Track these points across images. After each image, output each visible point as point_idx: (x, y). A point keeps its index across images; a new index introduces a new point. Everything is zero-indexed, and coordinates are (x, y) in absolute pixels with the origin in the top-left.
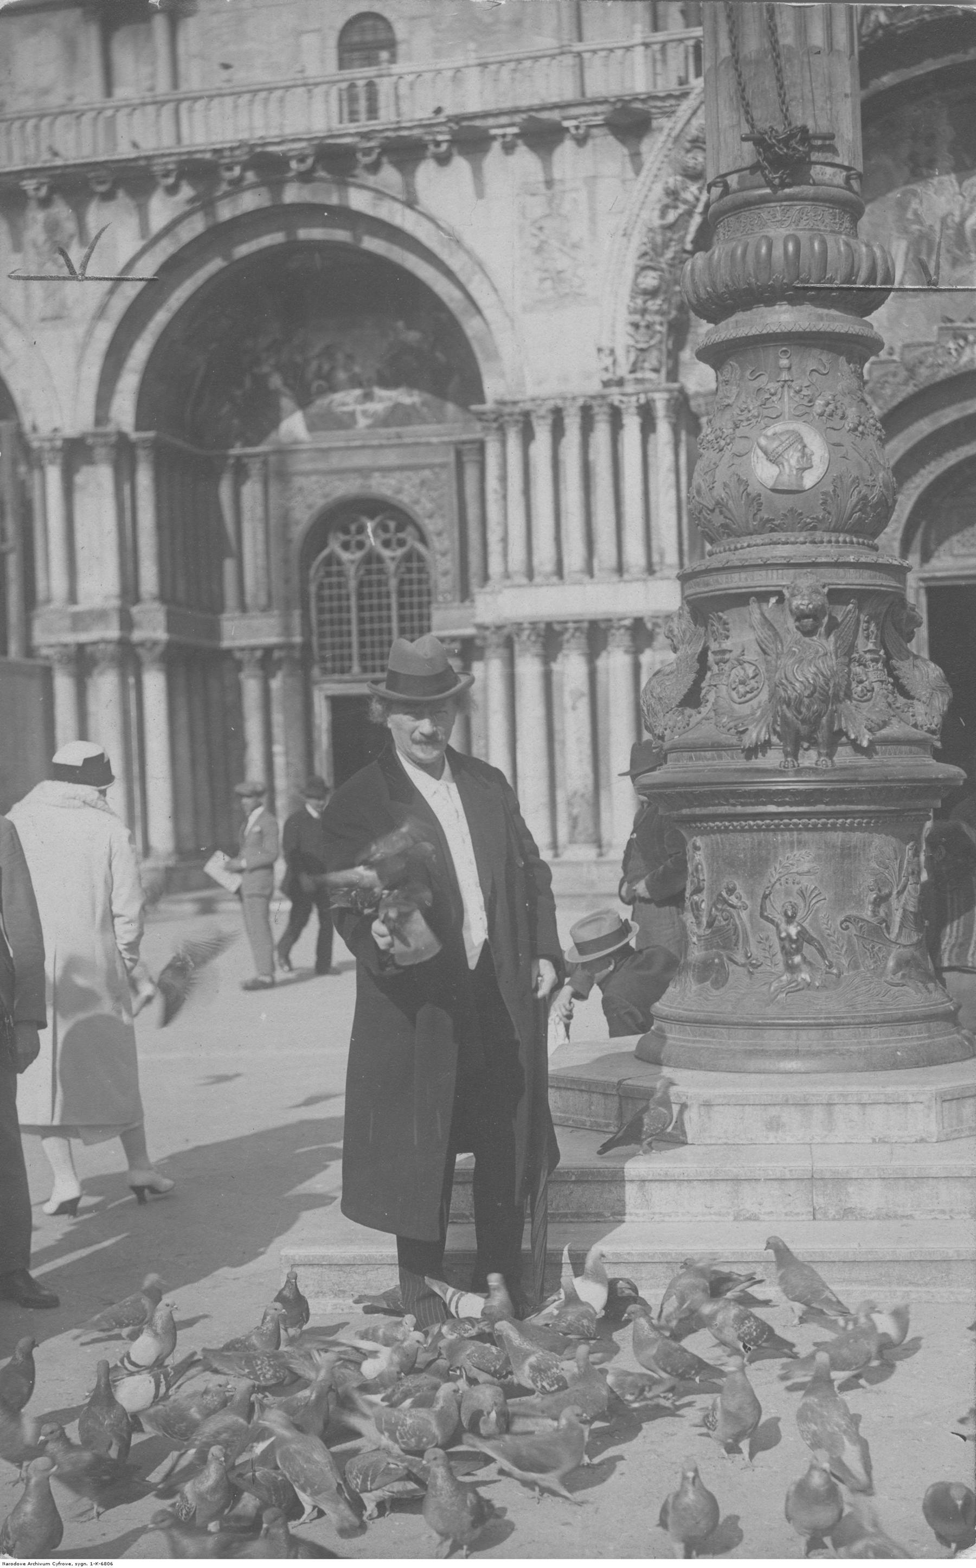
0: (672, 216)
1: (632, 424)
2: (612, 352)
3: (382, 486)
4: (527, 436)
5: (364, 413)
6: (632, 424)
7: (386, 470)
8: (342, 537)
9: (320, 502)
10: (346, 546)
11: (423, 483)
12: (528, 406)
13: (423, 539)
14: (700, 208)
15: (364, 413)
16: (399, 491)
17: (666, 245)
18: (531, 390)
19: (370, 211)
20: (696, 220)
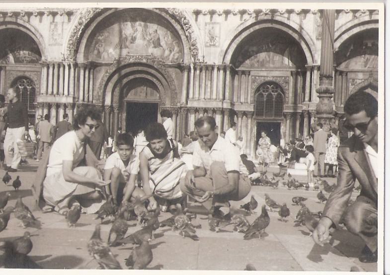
0: (75, 31)
1: (67, 68)
2: (64, 55)
3: (27, 74)
4: (48, 68)
5: (25, 60)
6: (67, 68)
7: (28, 71)
8: (20, 83)
9: (15, 76)
10: (20, 85)
11: (35, 74)
12: (48, 63)
13: (35, 85)
14: (81, 30)
15: (25, 60)
16: (30, 76)
17: (74, 36)
18: (49, 60)
19: (22, 24)
20: (80, 32)
